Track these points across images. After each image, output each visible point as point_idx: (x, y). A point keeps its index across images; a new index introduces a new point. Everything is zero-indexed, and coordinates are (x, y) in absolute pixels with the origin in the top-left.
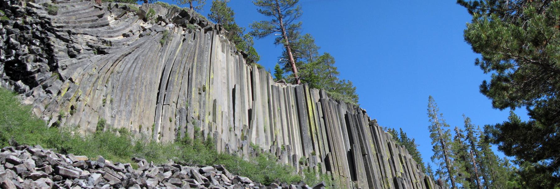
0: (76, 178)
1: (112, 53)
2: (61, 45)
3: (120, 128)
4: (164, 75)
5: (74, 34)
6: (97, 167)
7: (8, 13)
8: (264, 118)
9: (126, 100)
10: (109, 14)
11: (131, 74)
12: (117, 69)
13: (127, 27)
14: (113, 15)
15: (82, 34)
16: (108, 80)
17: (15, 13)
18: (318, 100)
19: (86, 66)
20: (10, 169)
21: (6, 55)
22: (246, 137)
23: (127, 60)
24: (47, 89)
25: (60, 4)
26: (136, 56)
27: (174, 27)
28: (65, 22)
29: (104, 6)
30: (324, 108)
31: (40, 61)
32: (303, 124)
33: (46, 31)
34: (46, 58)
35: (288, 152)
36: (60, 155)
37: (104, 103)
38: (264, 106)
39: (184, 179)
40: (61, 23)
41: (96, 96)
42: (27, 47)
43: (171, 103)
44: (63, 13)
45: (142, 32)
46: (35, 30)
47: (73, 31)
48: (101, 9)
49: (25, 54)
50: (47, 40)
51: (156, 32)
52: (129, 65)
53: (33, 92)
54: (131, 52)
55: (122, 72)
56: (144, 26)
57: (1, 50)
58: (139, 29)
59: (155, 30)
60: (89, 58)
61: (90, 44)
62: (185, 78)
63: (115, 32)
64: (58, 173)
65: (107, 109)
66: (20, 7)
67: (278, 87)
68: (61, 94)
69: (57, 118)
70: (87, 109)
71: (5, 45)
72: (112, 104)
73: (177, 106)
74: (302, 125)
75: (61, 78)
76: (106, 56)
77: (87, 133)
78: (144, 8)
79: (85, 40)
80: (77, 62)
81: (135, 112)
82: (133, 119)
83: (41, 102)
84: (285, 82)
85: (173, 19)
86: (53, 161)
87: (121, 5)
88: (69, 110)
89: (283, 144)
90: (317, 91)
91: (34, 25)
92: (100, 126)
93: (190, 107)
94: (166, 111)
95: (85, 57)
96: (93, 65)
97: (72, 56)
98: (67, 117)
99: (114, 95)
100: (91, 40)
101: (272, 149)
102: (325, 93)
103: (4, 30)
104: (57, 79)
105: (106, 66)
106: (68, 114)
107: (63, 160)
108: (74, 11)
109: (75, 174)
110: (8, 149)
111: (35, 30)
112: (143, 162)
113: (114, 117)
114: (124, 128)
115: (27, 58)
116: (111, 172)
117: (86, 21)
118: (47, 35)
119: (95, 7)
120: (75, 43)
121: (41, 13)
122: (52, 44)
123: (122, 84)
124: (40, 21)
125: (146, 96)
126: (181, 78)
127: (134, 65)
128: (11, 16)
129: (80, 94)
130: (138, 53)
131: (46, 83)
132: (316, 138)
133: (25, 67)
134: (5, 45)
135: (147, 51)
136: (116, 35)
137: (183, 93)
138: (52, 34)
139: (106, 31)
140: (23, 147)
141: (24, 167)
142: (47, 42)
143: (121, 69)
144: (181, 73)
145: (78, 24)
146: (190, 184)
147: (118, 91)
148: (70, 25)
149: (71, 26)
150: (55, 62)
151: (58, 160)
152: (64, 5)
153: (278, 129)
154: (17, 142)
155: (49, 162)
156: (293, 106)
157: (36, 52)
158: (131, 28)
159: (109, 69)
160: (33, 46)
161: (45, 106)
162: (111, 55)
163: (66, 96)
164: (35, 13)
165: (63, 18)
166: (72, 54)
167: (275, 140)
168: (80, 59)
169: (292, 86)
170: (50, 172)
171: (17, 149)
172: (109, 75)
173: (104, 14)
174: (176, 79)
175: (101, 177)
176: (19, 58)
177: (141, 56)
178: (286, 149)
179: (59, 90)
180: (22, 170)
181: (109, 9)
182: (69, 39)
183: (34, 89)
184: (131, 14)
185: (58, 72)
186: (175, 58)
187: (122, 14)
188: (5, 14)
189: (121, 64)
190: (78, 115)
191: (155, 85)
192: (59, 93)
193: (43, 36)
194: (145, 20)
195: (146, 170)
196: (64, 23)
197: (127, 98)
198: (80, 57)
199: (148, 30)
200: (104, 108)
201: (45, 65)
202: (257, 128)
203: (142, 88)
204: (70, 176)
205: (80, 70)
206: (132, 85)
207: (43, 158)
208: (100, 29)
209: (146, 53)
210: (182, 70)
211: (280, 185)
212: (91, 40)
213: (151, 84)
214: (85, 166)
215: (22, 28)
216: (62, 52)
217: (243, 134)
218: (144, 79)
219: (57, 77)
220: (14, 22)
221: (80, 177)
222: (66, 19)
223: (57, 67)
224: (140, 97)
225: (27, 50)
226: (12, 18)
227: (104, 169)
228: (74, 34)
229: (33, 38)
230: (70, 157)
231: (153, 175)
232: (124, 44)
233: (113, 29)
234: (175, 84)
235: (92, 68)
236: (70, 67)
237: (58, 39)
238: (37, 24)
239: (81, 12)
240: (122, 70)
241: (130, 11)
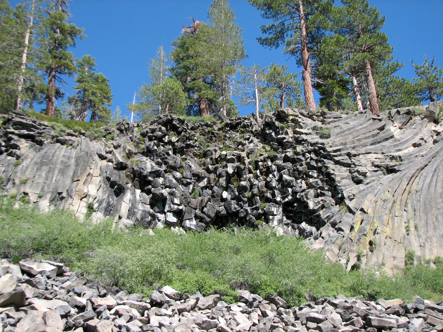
0: (393, 327)
2: (343, 171)
3: (433, 258)
5: (355, 156)
6: (416, 310)
7: (275, 146)
10: (391, 123)
11: (432, 190)
12: (415, 187)
13: (416, 134)
14: (397, 124)
15: (364, 154)
16: (406, 202)
17: (283, 145)
19: (376, 191)
20: (314, 329)
21: (281, 195)
23: (424, 174)
24: (336, 227)
25: (332, 124)
26: (435, 167)
28: (342, 144)
29: (383, 115)
31: (323, 195)
33: (322, 159)
34: (328, 190)
36: (368, 302)
37: (408, 231)
41: (396, 224)
42: (303, 182)
44: (338, 134)
45: (435, 137)
46: (308, 160)
47: (353, 152)
48: (380, 120)
49: (304, 191)
50: (325, 169)
52: (428, 180)
53: (321, 233)
54: (427, 163)
55: (421, 190)
56: (436, 129)
57: (275, 191)
60: (378, 181)
61: (376, 164)
63: (402, 144)
64: (371, 326)
65: (413, 237)
66: (287, 137)
68: (354, 230)
69: (356, 259)
70: (388, 241)
71: (279, 184)
72: (417, 231)
75: (350, 211)
76: (398, 174)
77: (395, 271)
78: (432, 108)
79: (369, 160)
80: (365, 188)
83: (333, 243)
86: (362, 311)
87: (403, 110)
88: (368, 246)
91: (307, 154)
92: (409, 260)
95: (374, 181)
96: (384, 188)
97: (358, 182)
98: (367, 255)
99: (418, 219)
100: (376, 158)
103: (274, 167)
104: (346, 212)
105: (401, 186)
106: (367, 252)
107: (372, 308)
108: (349, 129)
109: (390, 323)
110: (306, 305)
111: (308, 160)
113: (423, 246)
114: (439, 258)
115: (306, 195)
116: (434, 315)
117: (366, 138)
118: (325, 163)
119: (373, 119)
120: (358, 166)
121: (312, 139)
122: (332, 172)
123: (425, 205)
124: (312, 148)
128: (278, 149)
129: (376, 225)
130: (437, 163)
131: (334, 220)
133: (306, 206)
134: (279, 184)
136: (405, 147)
138: (329, 161)
140: (323, 301)
141: (329, 324)
142: (325, 171)
143: (420, 186)
145: (357, 144)
147: (421, 214)
148: (348, 146)
150: (339, 193)
151: (367, 309)
152: (336, 124)
154: (316, 296)
155: (357, 314)
157: (315, 185)
158: (421, 135)
159: (405, 190)
160: (311, 179)
161: (338, 247)
162: (403, 173)
163: (360, 231)
164: (306, 140)
165: (338, 140)
168: (367, 184)
170: (361, 324)
171: (316, 304)
172: (406, 196)
175: (424, 322)
176: (298, 197)
179: (352, 226)
180: (328, 328)
181: (390, 117)
182: (350, 162)
183: (321, 229)
184: (418, 118)
185: (345, 204)
187: (407, 121)
188: (271, 149)
189: (418, 181)
190: (380, 250)
192: (352, 228)
193: (320, 165)
194: (436, 122)
196: (340, 145)
197: (434, 220)
198: (368, 181)
200: (408, 237)
201: (329, 199)
204: (385, 327)
205: (370, 197)
206: (437, 203)
207: (349, 310)
208: (384, 144)
212: (376, 158)
214: (401, 311)
215: (293, 161)
219: (346, 210)
220: (283, 155)
221: (398, 325)
223: (343, 198)
225: (304, 186)
226: (280, 152)
227: (426, 312)
228: (355, 156)
229: (308, 169)
230: (380, 303)
232: (416, 157)
233: (399, 141)
235: (384, 192)
236: (358, 196)
237: (338, 166)
238: (309, 152)
239: (357, 129)
240: (421, 187)
241: (416, 116)
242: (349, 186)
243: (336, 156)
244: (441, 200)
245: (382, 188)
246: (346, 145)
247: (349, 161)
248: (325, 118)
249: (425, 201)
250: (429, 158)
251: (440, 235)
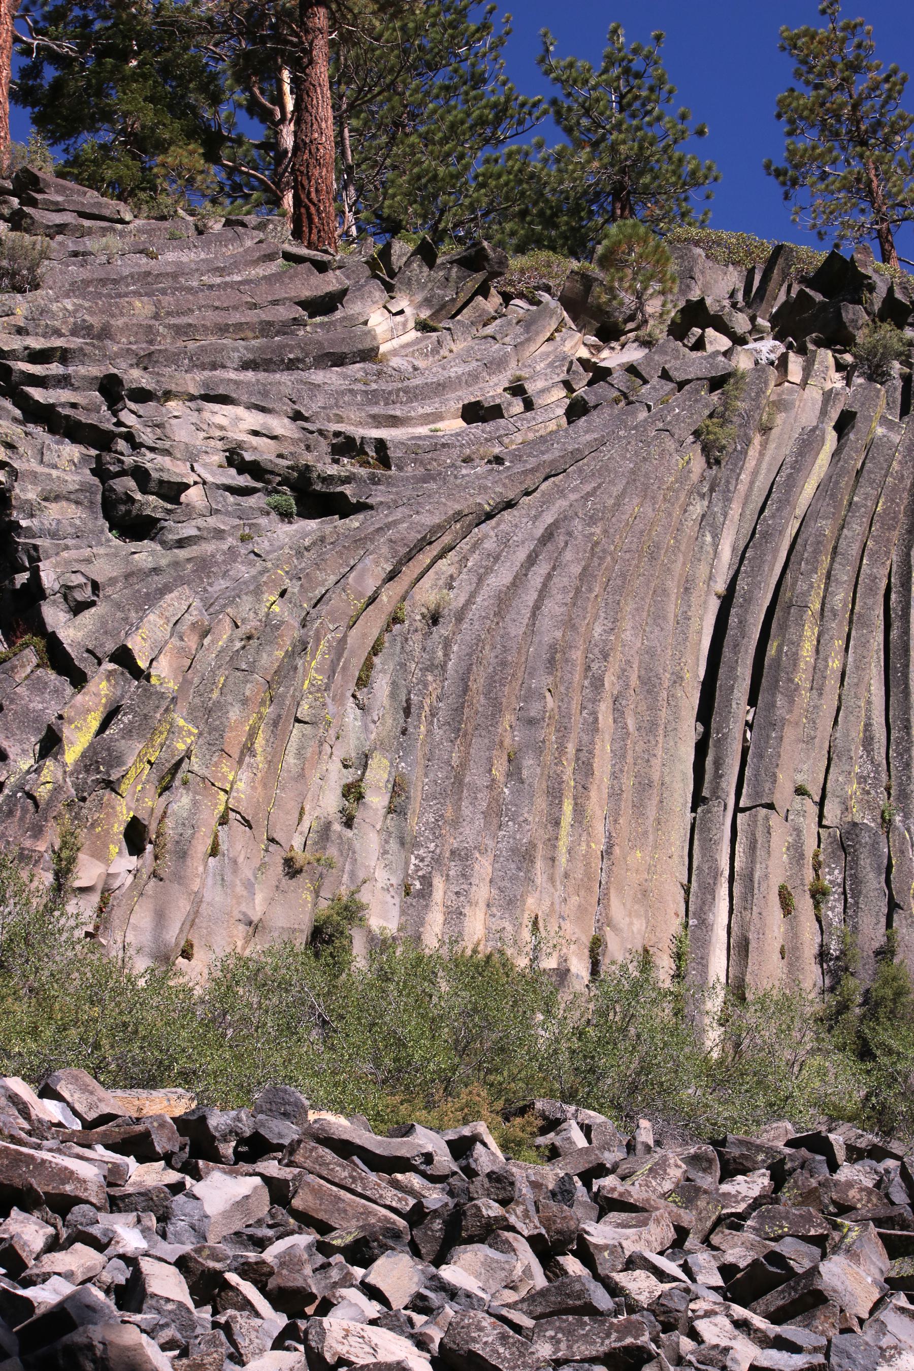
0: (78, 1201)
1: (395, 505)
2: (63, 463)
4: (730, 632)
5: (142, 396)
9: (490, 787)
10: (379, 294)
11: (516, 628)
13: (495, 365)
15: (192, 398)
16: (368, 666)
23: (489, 545)
26: (548, 518)
27: (784, 359)
39: (853, 1215)
40: (58, 333)
41: (291, 759)
43: (783, 795)
47: (136, 377)
51: (671, 385)
52: (501, 577)
54: (511, 495)
55: (460, 617)
58: (563, 376)
59: (665, 375)
61: (248, 456)
62: (865, 645)
63: (415, 395)
73: (821, 816)
76: (355, 522)
79: (218, 433)
80: (163, 562)
81: (553, 859)
82: (548, 903)
85: (774, 319)
93: (906, 817)
94: (752, 847)
95: (219, 534)
96: (262, 573)
100: (255, 433)
105: (352, 577)
109: (68, 1175)
112: (587, 1130)
119: (288, 256)
120: (152, 449)
125: (624, 756)
126: (839, 643)
127: (542, 569)
129: (181, 746)
130: (561, 504)
135: (616, 490)
136: (421, 411)
137: (857, 734)
139: (359, 386)
143: (457, 598)
144: (835, 614)
145: (166, 343)
146: (879, 1234)
149: (117, 355)
152: (90, 244)
159: (373, 600)
166: (129, 512)
168: (181, 543)
172: (375, 633)
173: (344, 292)
174: (807, 650)
177: (577, 525)
179: (50, 728)
182: (108, 425)
185: (42, 623)
186: (791, 531)
187: (463, 298)
189: (452, 570)
191: (679, 694)
195: (600, 1170)
196: (74, 333)
198: (188, 530)
199: (618, 378)
200: (349, 833)
203: (594, 714)
206: (530, 695)
208: (318, 376)
209: (611, 502)
210: (840, 598)
212: (255, 433)
213: (649, 684)
216: (64, 503)
218: (606, 657)
222: (90, 311)
224: (585, 768)
228: (142, 396)
230: (63, 1089)
231: (636, 1192)
234: (802, 677)
235: (257, 592)
237: (38, 431)
242: (83, 542)
243: (40, 382)
244: (550, 679)
245: (253, 571)
246: (108, 342)
247: (104, 419)
248: (34, 203)
249: (469, 670)
250: (525, 473)
251: (514, 851)
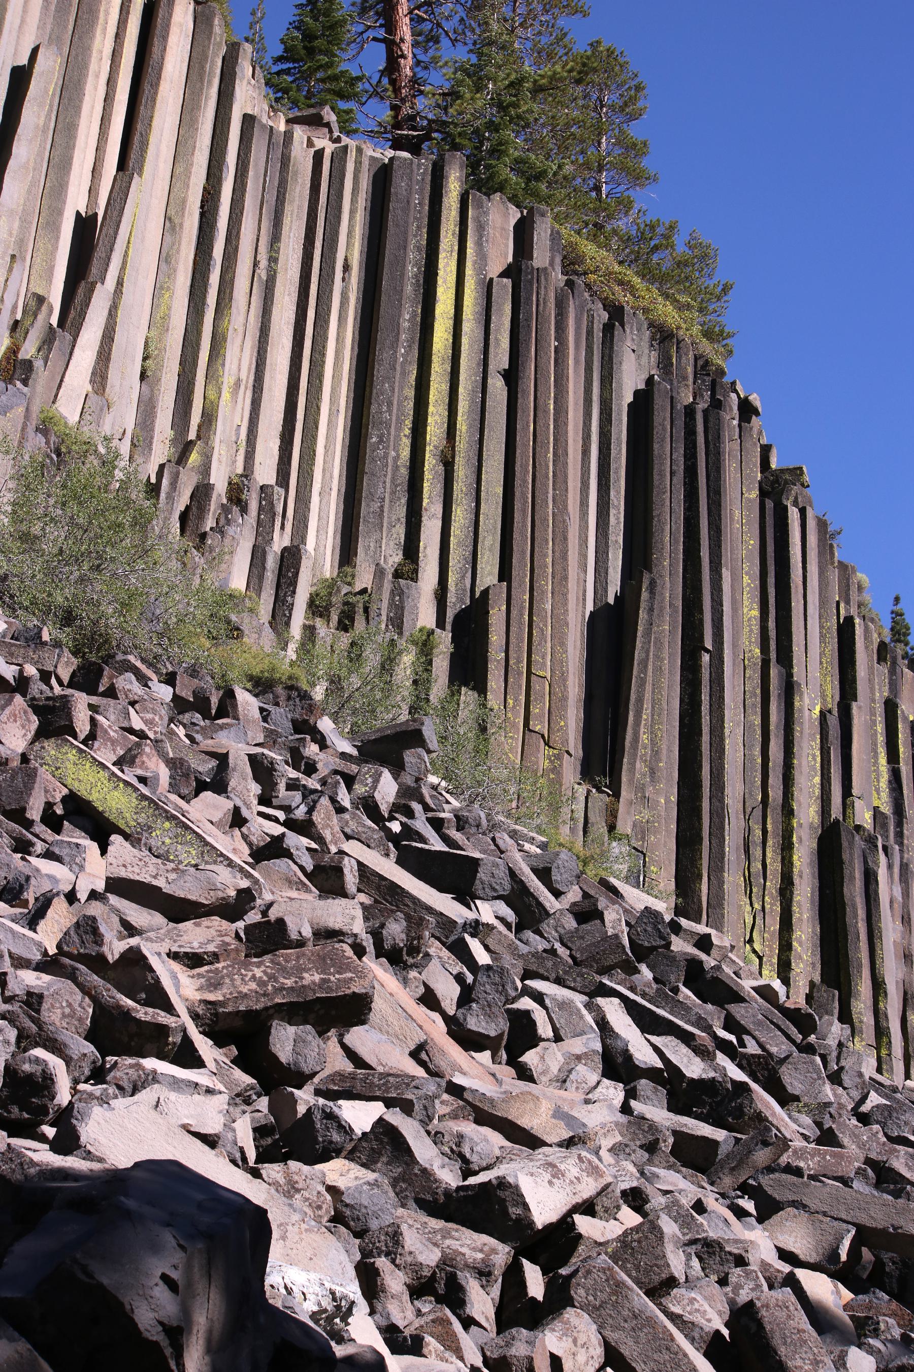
8: (159, 290)
18: (500, 269)
22: (28, 365)
30: (528, 320)
32: (380, 385)
35: (259, 523)
38: (171, 224)
67: (288, 137)
74: (377, 388)
84: (335, 127)
89: (240, 470)
90: (506, 215)
101: (165, 482)
102: (555, 237)
132: (439, 488)
153: (232, 380)
156: (346, 268)
167: (199, 437)
169: (370, 151)
178: (253, 506)
202: (108, 337)
211: (170, 680)
217: (13, 350)
